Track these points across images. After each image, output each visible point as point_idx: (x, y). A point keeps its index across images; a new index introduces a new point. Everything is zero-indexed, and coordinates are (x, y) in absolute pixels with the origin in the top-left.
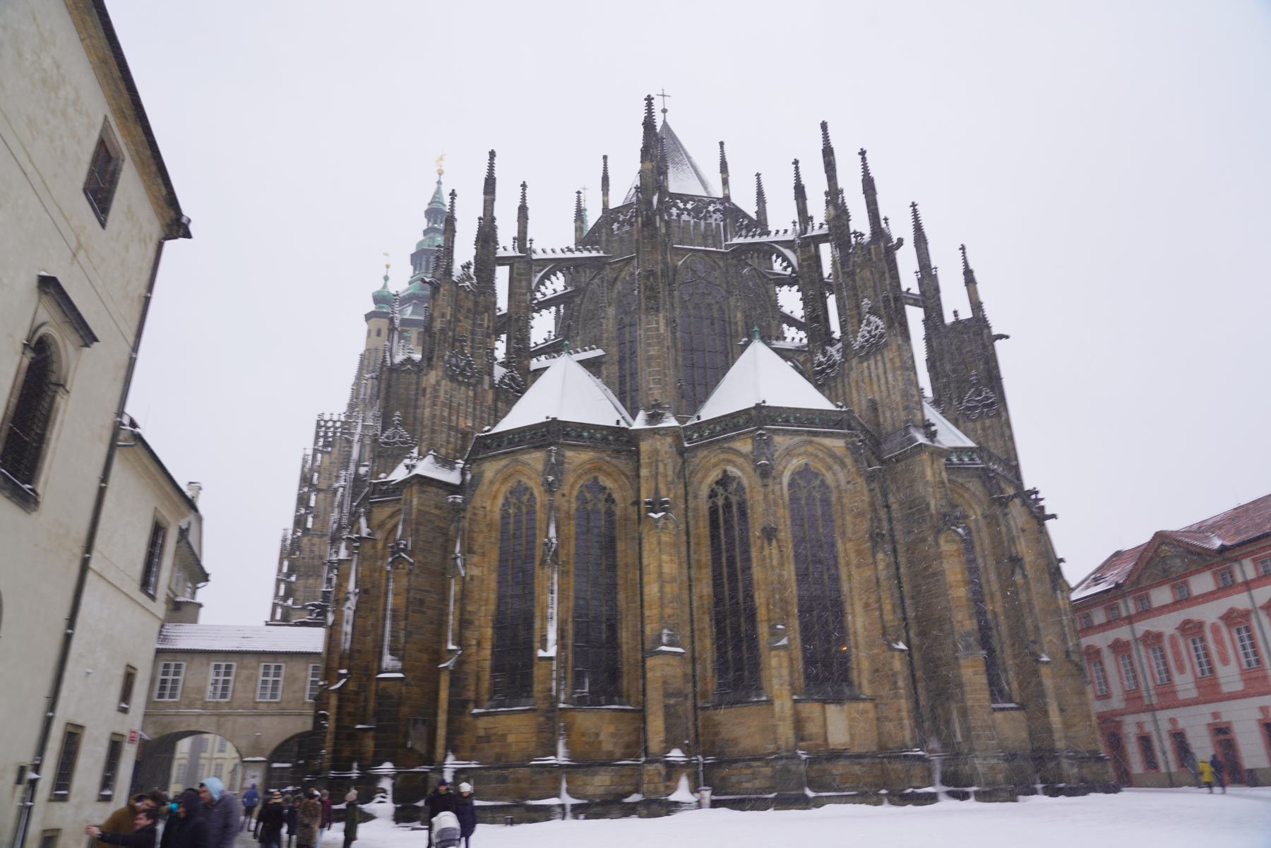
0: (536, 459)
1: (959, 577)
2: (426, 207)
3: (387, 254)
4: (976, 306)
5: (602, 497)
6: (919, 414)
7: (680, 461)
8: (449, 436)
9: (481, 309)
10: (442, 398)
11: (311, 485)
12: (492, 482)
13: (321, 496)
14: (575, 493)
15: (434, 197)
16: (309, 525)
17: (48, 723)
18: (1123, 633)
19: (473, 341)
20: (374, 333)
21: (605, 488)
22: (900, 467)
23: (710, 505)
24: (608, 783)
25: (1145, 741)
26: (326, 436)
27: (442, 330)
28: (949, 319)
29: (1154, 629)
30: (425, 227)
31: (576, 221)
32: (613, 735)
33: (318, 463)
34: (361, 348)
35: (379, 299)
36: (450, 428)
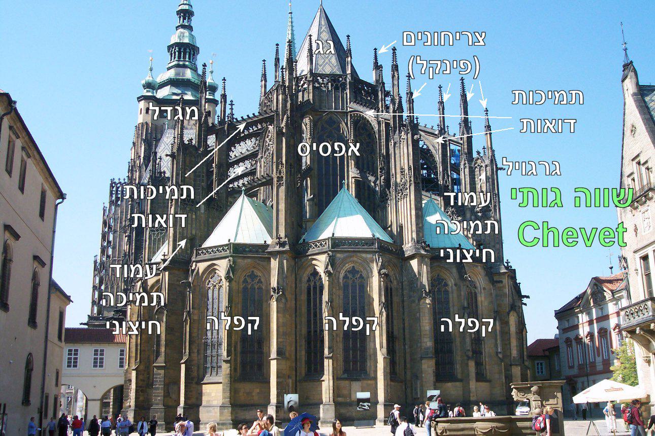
12: (204, 273)
17: (43, 392)
23: (307, 285)
26: (117, 193)
32: (258, 393)
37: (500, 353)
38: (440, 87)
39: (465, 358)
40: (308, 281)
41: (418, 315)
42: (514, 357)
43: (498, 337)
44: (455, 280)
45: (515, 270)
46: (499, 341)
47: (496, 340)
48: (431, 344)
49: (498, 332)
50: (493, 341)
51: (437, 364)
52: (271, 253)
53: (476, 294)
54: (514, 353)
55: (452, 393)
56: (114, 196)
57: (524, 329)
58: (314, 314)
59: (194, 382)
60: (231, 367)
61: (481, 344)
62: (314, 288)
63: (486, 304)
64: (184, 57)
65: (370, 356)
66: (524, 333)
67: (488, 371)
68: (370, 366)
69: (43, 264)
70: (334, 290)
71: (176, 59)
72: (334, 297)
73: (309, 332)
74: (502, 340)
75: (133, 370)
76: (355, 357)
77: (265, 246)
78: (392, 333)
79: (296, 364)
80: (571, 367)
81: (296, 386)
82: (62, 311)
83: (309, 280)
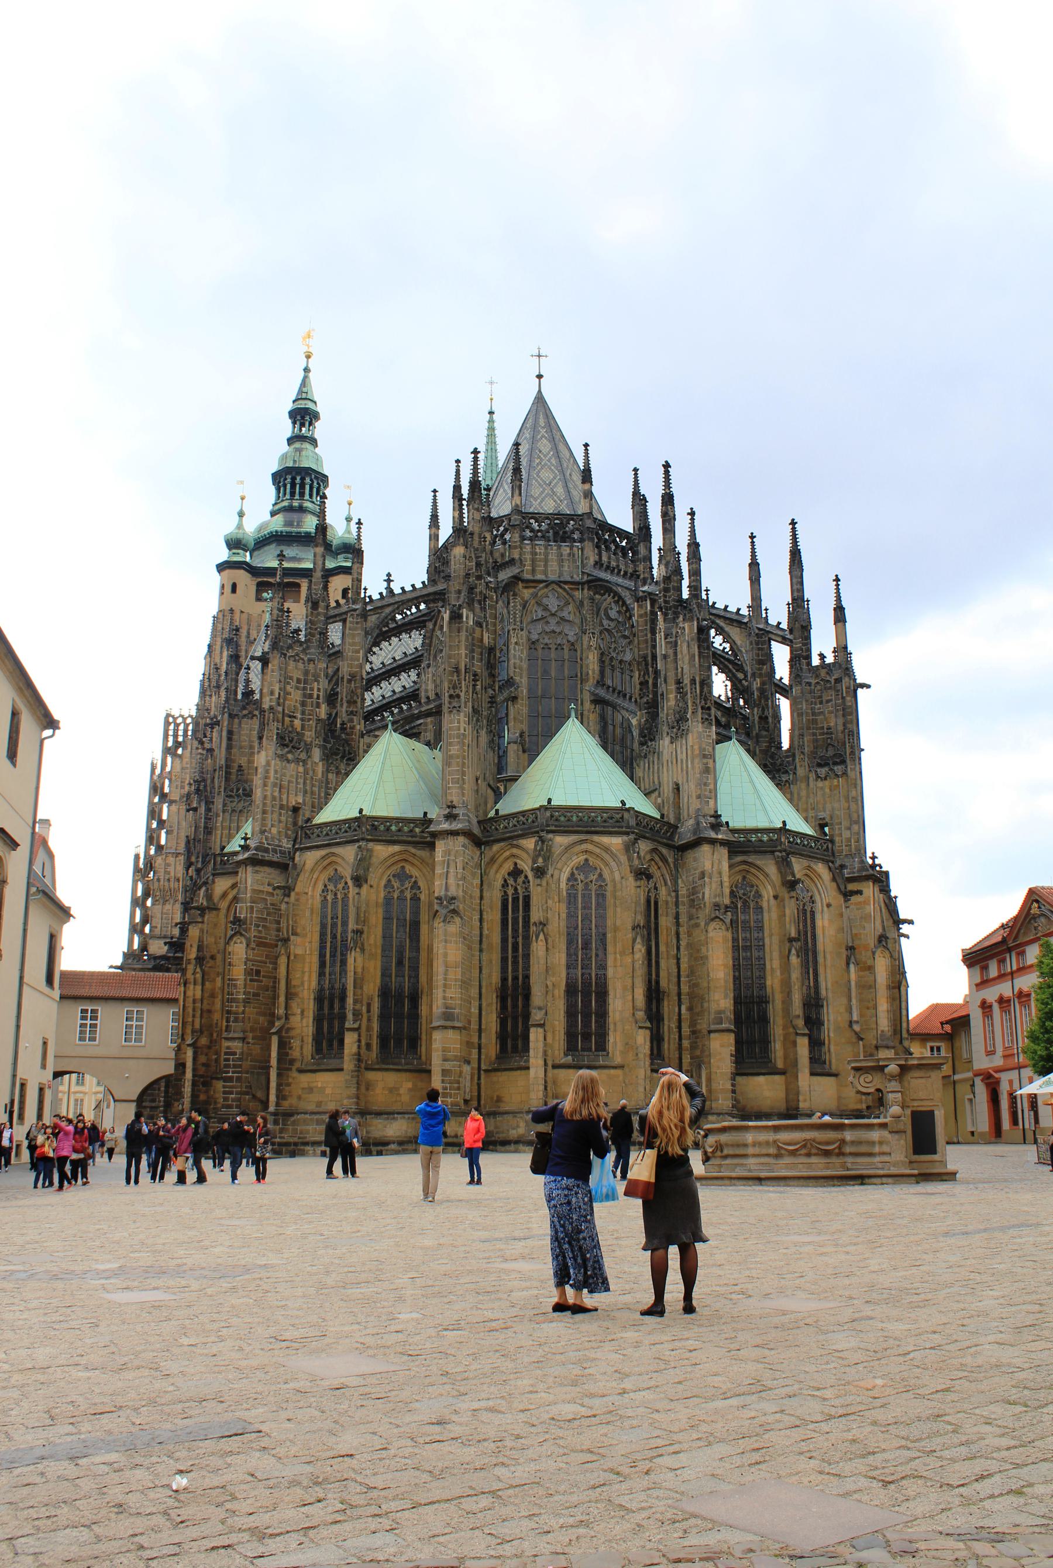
0: (349, 853)
1: (720, 962)
2: (290, 406)
3: (242, 482)
4: (842, 650)
5: (407, 885)
6: (712, 802)
7: (478, 853)
8: (280, 814)
9: (310, 677)
10: (272, 779)
11: (164, 797)
13: (174, 807)
14: (383, 882)
15: (300, 392)
16: (163, 842)
17: (14, 1076)
18: (1005, 989)
19: (303, 713)
20: (228, 589)
21: (411, 877)
22: (690, 855)
24: (404, 1128)
25: (1013, 1099)
26: (176, 736)
27: (271, 708)
28: (816, 661)
29: (1025, 989)
30: (289, 434)
31: (430, 527)
32: (410, 1090)
33: (168, 769)
34: (215, 612)
35: (234, 544)
36: (282, 807)
37: (857, 1022)
38: (752, 537)
39: (791, 1030)
40: (503, 886)
41: (704, 949)
42: (883, 1031)
43: (853, 994)
44: (774, 887)
45: (887, 873)
46: (854, 1001)
47: (850, 1000)
48: (728, 1005)
49: (853, 983)
50: (844, 1000)
51: (738, 1043)
52: (435, 835)
53: (813, 913)
54: (884, 1024)
55: (767, 1093)
56: (171, 739)
57: (904, 982)
58: (513, 944)
59: (294, 1068)
60: (359, 1041)
61: (822, 1006)
62: (513, 899)
63: (831, 932)
64: (302, 494)
65: (615, 1024)
66: (902, 988)
67: (833, 1055)
68: (615, 1042)
69: (14, 845)
70: (550, 902)
71: (288, 496)
72: (549, 915)
73: (504, 980)
74: (861, 1001)
75: (188, 1045)
76: (587, 1023)
77: (426, 821)
78: (658, 982)
79: (480, 1037)
80: (990, 1053)
81: (479, 1078)
82: (54, 933)
83: (505, 884)
